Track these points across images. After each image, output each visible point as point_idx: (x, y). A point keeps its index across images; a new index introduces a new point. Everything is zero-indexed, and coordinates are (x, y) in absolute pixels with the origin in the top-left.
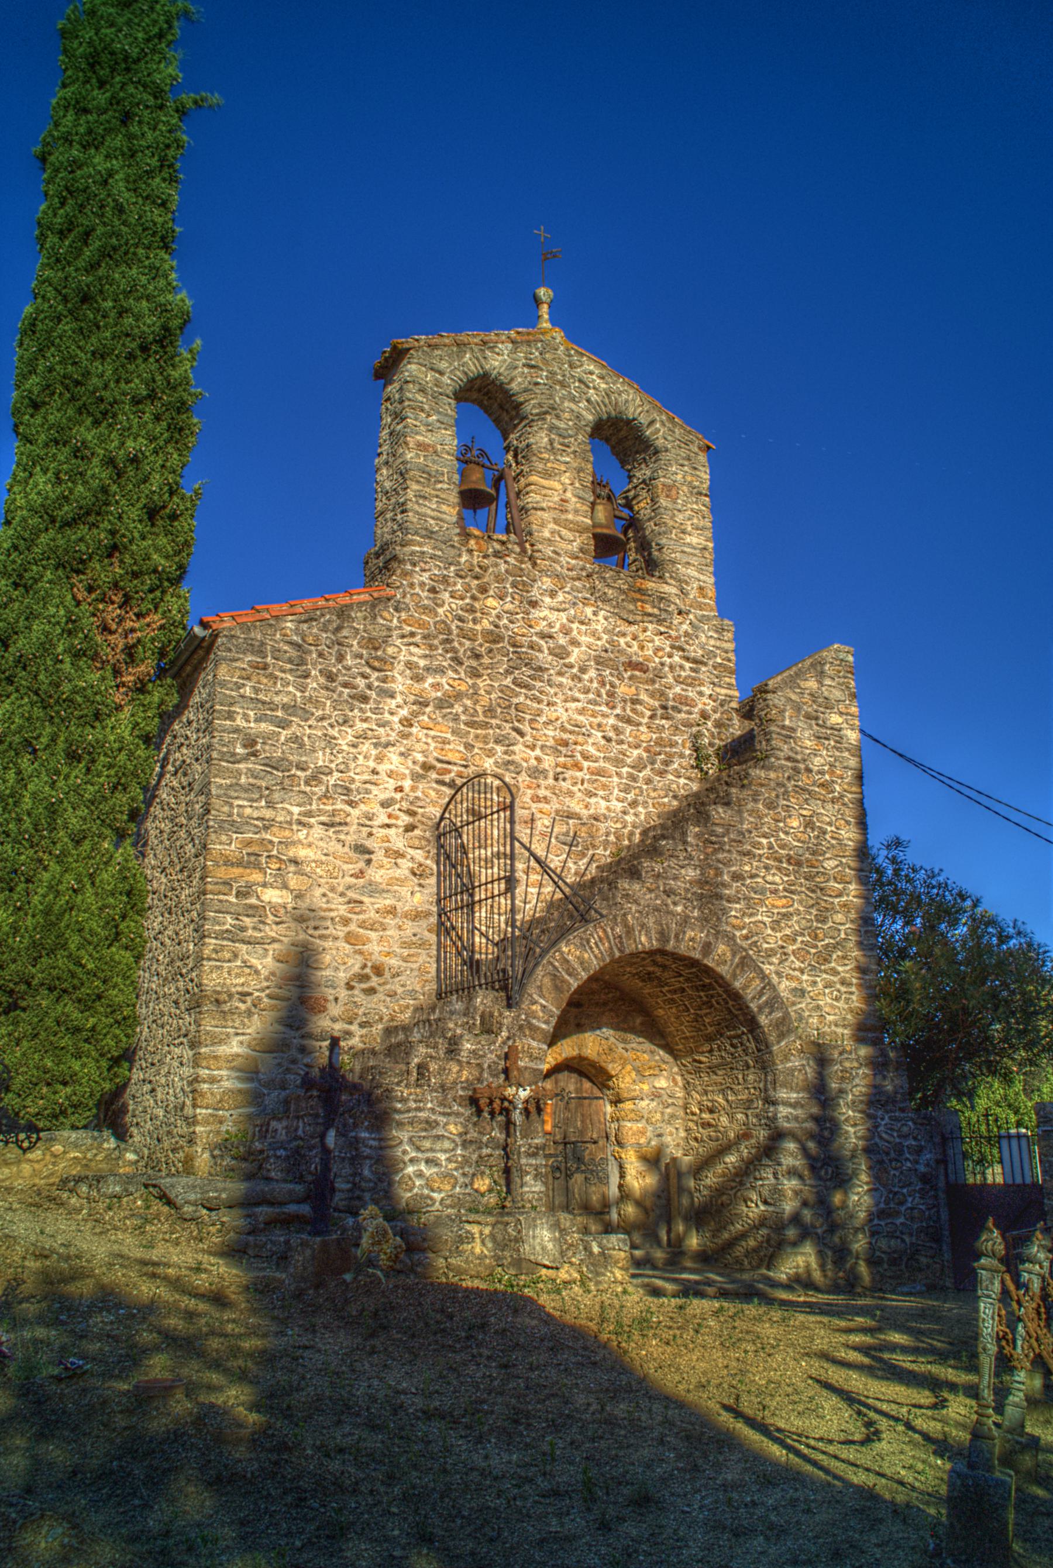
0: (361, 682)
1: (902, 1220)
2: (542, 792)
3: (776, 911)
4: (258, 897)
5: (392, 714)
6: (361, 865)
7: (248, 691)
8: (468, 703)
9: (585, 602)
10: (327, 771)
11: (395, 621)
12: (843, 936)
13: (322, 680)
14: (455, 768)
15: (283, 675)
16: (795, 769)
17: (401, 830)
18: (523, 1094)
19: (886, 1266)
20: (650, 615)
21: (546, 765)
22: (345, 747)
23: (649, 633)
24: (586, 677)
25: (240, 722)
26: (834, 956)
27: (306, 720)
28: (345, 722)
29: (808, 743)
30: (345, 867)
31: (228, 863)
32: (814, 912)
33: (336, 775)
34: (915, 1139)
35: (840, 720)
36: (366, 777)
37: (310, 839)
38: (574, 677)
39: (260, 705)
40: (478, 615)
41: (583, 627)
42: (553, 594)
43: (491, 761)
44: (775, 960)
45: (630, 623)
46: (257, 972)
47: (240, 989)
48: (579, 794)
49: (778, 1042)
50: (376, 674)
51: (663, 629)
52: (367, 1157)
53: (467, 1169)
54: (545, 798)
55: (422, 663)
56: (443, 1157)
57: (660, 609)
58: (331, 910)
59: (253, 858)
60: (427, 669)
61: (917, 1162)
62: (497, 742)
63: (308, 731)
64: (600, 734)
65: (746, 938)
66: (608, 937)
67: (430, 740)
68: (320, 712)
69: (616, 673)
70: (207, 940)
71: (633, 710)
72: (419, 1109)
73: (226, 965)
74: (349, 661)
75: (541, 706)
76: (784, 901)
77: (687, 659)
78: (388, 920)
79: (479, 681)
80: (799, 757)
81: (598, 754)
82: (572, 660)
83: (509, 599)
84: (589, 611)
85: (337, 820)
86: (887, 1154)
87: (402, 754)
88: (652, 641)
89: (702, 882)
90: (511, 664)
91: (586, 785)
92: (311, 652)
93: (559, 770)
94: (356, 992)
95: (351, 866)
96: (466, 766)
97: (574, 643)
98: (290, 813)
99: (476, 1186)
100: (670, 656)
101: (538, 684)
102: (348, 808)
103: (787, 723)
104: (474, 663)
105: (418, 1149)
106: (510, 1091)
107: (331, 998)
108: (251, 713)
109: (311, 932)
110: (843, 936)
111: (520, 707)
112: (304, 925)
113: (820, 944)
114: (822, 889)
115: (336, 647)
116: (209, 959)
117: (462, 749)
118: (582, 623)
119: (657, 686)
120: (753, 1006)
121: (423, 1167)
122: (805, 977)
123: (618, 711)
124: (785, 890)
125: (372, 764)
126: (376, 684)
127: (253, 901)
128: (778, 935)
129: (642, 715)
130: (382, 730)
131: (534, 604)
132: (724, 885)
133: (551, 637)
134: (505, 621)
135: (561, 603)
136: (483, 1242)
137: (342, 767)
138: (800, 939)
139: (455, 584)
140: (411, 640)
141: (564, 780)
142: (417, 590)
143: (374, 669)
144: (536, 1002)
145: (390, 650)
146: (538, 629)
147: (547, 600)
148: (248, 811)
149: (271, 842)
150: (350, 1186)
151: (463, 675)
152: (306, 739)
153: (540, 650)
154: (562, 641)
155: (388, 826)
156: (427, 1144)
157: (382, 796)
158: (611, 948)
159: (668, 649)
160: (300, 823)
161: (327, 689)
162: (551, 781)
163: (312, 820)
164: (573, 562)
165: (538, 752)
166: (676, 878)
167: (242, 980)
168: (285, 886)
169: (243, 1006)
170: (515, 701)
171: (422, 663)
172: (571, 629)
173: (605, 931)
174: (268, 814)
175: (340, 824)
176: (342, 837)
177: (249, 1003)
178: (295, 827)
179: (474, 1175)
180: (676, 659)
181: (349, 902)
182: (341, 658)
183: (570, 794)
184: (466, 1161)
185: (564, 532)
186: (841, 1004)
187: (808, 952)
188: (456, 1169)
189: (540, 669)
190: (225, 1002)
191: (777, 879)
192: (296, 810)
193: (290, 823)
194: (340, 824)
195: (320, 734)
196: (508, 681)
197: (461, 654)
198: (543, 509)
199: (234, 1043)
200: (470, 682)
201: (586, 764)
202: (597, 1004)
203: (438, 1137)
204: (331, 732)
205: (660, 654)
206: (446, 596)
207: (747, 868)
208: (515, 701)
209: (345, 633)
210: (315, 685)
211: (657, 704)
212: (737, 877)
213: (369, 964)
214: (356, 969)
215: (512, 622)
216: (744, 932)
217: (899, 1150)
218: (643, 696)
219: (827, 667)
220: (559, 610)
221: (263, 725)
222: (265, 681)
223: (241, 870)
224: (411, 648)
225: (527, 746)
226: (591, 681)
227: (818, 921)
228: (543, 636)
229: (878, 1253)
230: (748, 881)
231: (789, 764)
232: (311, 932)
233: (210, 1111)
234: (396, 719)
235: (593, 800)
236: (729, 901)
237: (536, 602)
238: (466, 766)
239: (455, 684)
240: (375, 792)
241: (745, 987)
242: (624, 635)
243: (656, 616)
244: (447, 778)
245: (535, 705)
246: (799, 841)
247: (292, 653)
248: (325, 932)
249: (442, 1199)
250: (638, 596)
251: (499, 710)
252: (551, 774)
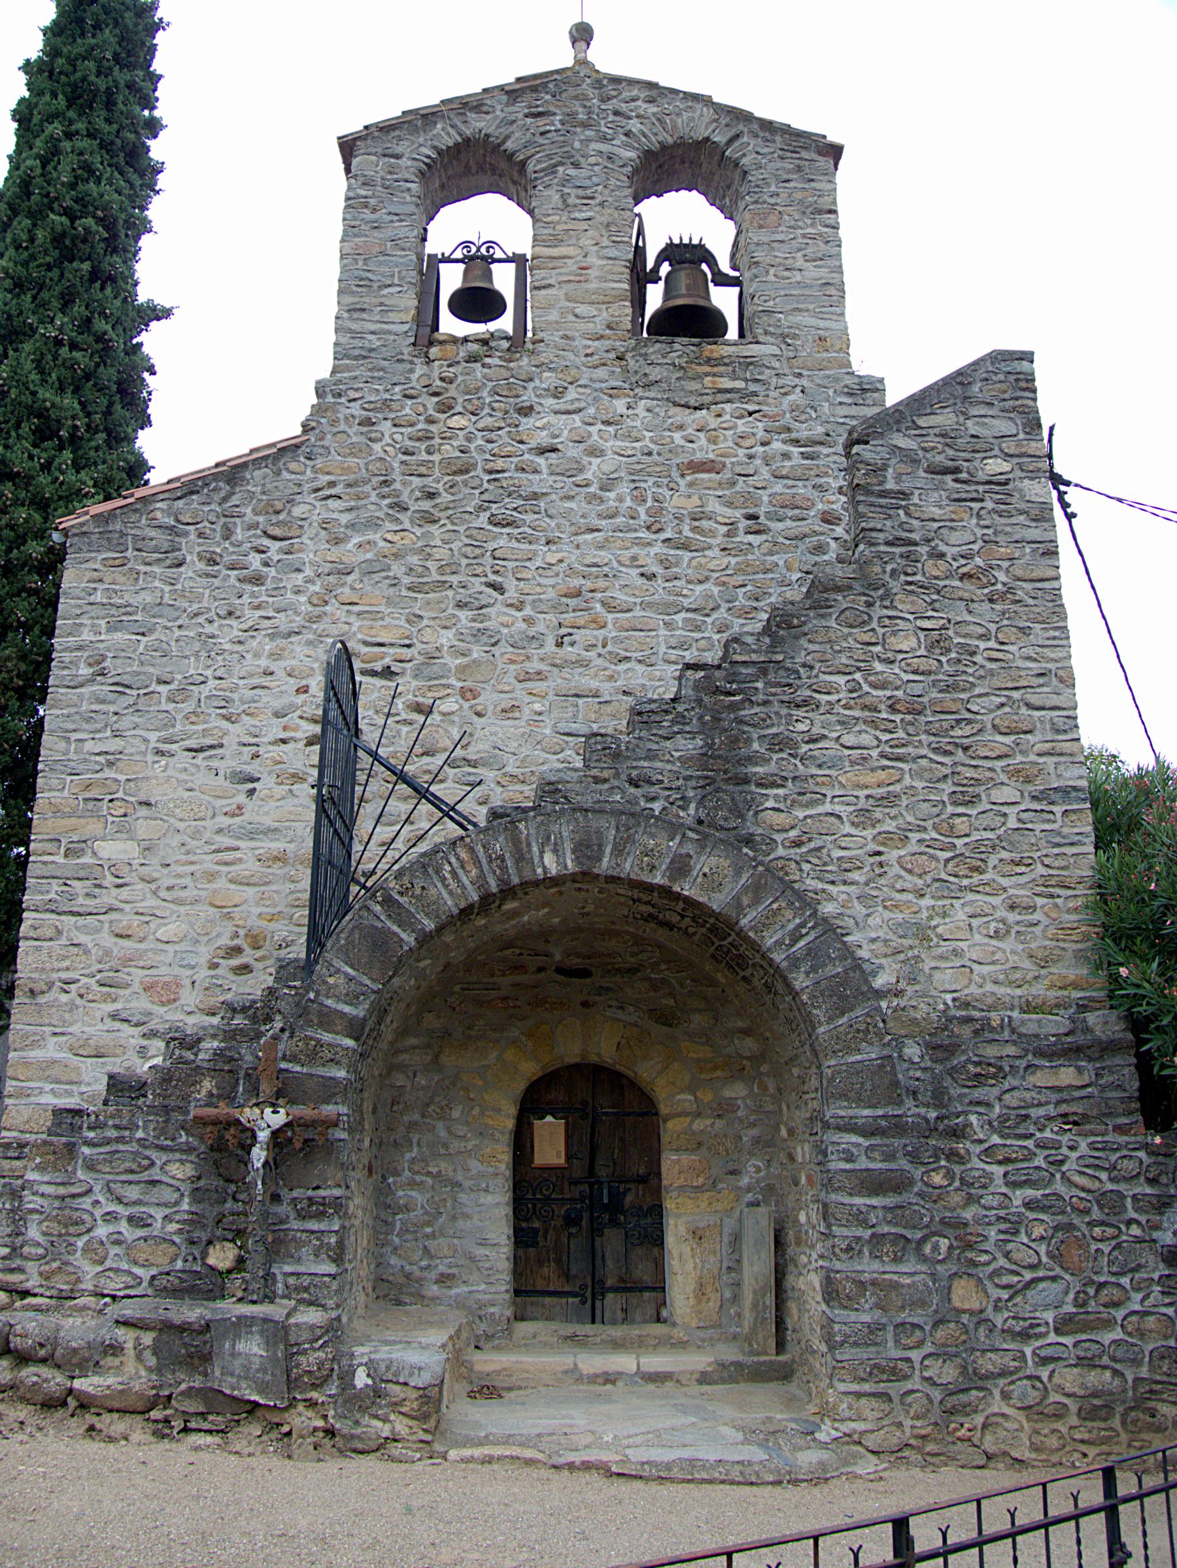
0: (255, 560)
1: (1117, 1334)
2: (535, 665)
3: (862, 793)
4: (95, 854)
5: (298, 592)
6: (242, 798)
7: (98, 597)
8: (414, 560)
9: (613, 393)
10: (202, 679)
11: (309, 472)
12: (1012, 823)
13: (201, 566)
14: (392, 651)
15: (148, 569)
16: (906, 556)
17: (301, 744)
18: (278, 1119)
19: (1074, 1420)
21: (540, 627)
22: (227, 646)
23: (727, 417)
24: (612, 495)
25: (87, 636)
26: (993, 860)
27: (175, 620)
28: (230, 614)
29: (937, 512)
30: (219, 803)
31: (57, 812)
32: (948, 787)
33: (212, 683)
34: (1152, 1181)
35: (1006, 467)
36: (255, 681)
37: (170, 772)
38: (591, 499)
39: (113, 611)
40: (437, 441)
41: (611, 429)
42: (557, 393)
43: (450, 634)
44: (855, 876)
45: (696, 408)
46: (87, 952)
47: (64, 975)
48: (600, 661)
49: (831, 1019)
50: (278, 544)
51: (751, 408)
52: (32, 1211)
53: (196, 1234)
54: (539, 673)
55: (344, 518)
56: (159, 1214)
57: (746, 380)
58: (192, 863)
59: (91, 804)
60: (351, 526)
61: (1157, 1227)
62: (460, 605)
63: (177, 633)
64: (635, 572)
65: (798, 844)
66: (477, 862)
67: (352, 619)
68: (195, 606)
69: (666, 481)
71: (694, 529)
72: (120, 1140)
73: (45, 944)
74: (239, 534)
75: (533, 547)
76: (882, 775)
77: (796, 442)
78: (277, 869)
79: (433, 528)
80: (915, 536)
81: (633, 600)
82: (589, 475)
83: (487, 410)
84: (620, 405)
85: (208, 741)
86: (1087, 1212)
87: (310, 643)
88: (735, 427)
89: (705, 758)
90: (486, 497)
91: (609, 648)
92: (187, 534)
93: (564, 631)
94: (219, 971)
95: (225, 802)
96: (409, 646)
97: (595, 452)
98: (146, 740)
99: (211, 1261)
100: (763, 444)
101: (529, 517)
102: (225, 724)
103: (890, 485)
104: (426, 505)
105: (119, 1200)
106: (248, 1114)
107: (187, 982)
108: (103, 623)
109: (163, 894)
110: (1012, 823)
111: (498, 554)
112: (153, 886)
113: (959, 842)
114: (966, 749)
115: (223, 520)
116: (26, 938)
117: (402, 623)
118: (607, 423)
119: (738, 488)
120: (778, 957)
121: (123, 1226)
122: (927, 901)
124: (883, 755)
125: (264, 662)
126: (276, 558)
127: (87, 859)
128: (869, 833)
129: (712, 533)
130: (282, 615)
131: (526, 411)
132: (751, 760)
134: (480, 442)
135: (572, 402)
136: (139, 1357)
137: (219, 673)
138: (914, 836)
139: (403, 408)
140: (333, 491)
141: (572, 644)
142: (342, 427)
143: (275, 538)
144: (338, 971)
145: (297, 511)
146: (533, 444)
147: (550, 402)
148: (89, 746)
149: (116, 780)
150: (7, 1250)
151: (407, 525)
152: (173, 643)
153: (536, 471)
154: (573, 451)
155: (284, 741)
156: (133, 1193)
157: (277, 704)
158: (482, 876)
159: (761, 434)
160: (160, 753)
161: (207, 575)
162: (550, 646)
163: (174, 747)
164: (596, 343)
165: (528, 611)
166: (651, 756)
167: (67, 963)
168: (131, 836)
169: (64, 998)
170: (491, 546)
171: (344, 518)
172: (590, 435)
173: (472, 850)
174: (114, 745)
175: (212, 747)
176: (215, 763)
177: (74, 994)
178: (150, 758)
179: (210, 1242)
180: (777, 445)
181: (218, 851)
182: (228, 534)
183: (584, 664)
184: (195, 1221)
185: (581, 309)
186: (1008, 944)
187: (933, 857)
188: (180, 1232)
189: (535, 496)
190: (43, 992)
191: (866, 739)
192: (153, 736)
193: (144, 753)
194: (212, 747)
195: (192, 634)
196: (483, 520)
197: (405, 497)
198: (550, 286)
199: (51, 1046)
200: (418, 531)
201: (610, 616)
202: (619, 970)
203: (153, 1183)
204: (209, 629)
205: (748, 443)
206: (386, 427)
207: (801, 727)
208: (491, 546)
209: (235, 500)
210: (191, 574)
211: (738, 514)
212: (778, 744)
213: (242, 932)
214: (225, 941)
215: (489, 441)
216: (793, 834)
217: (1111, 1203)
218: (714, 506)
219: (976, 388)
220: (568, 412)
221: (118, 635)
222: (123, 579)
223: (73, 820)
224: (330, 502)
225: (511, 605)
226: (621, 500)
227: (955, 803)
228: (542, 451)
229: (1054, 1397)
230: (805, 748)
231: (897, 550)
232: (163, 894)
233: (15, 1134)
234: (303, 599)
235: (622, 667)
236: (759, 785)
237: (531, 408)
238: (409, 646)
239: (396, 538)
240: (265, 699)
241: (762, 926)
242: (681, 427)
243: (738, 391)
244: (378, 666)
245: (527, 546)
246: (915, 672)
247: (162, 539)
248: (183, 894)
249: (153, 1277)
250: (707, 369)
251: (464, 562)
252: (550, 641)
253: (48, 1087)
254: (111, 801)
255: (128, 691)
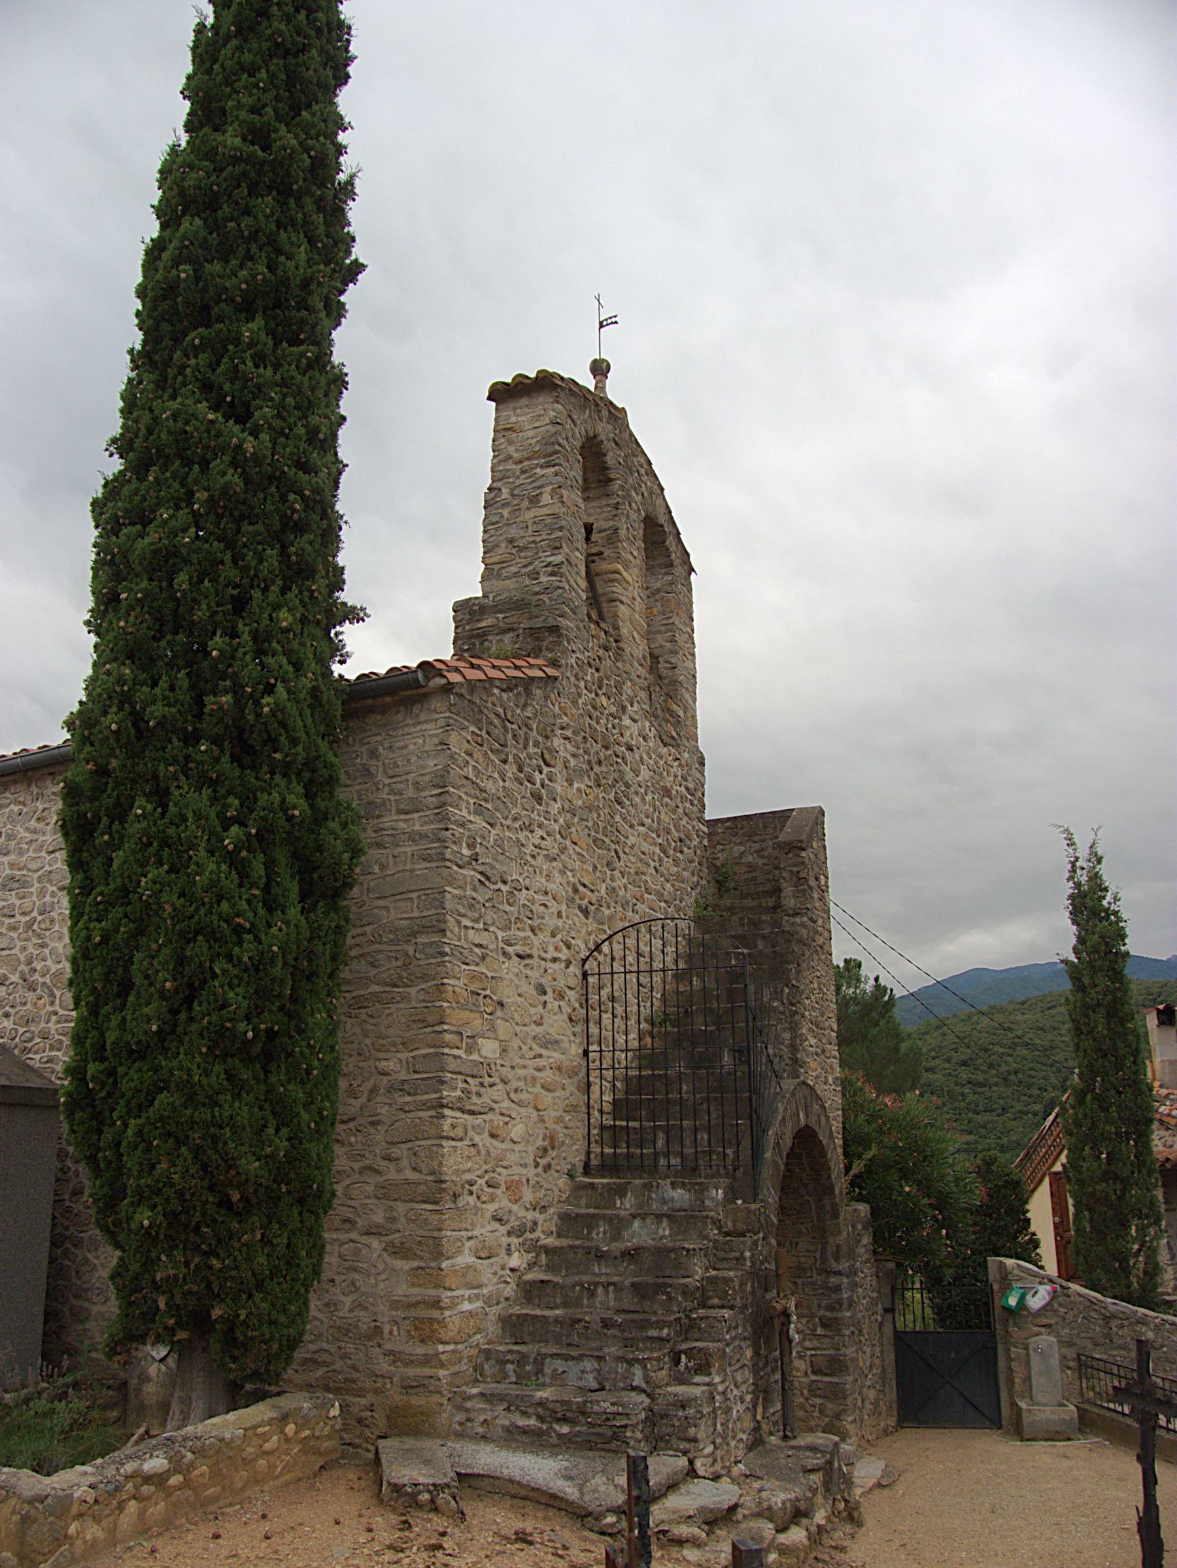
17: (563, 964)
20: (673, 737)
39: (478, 793)
70: (447, 1112)
116: (448, 1138)
123: (660, 841)
133: (632, 750)
176: (529, 973)
192: (500, 934)
253: (467, 1293)
254: (485, 997)
255: (487, 883)
